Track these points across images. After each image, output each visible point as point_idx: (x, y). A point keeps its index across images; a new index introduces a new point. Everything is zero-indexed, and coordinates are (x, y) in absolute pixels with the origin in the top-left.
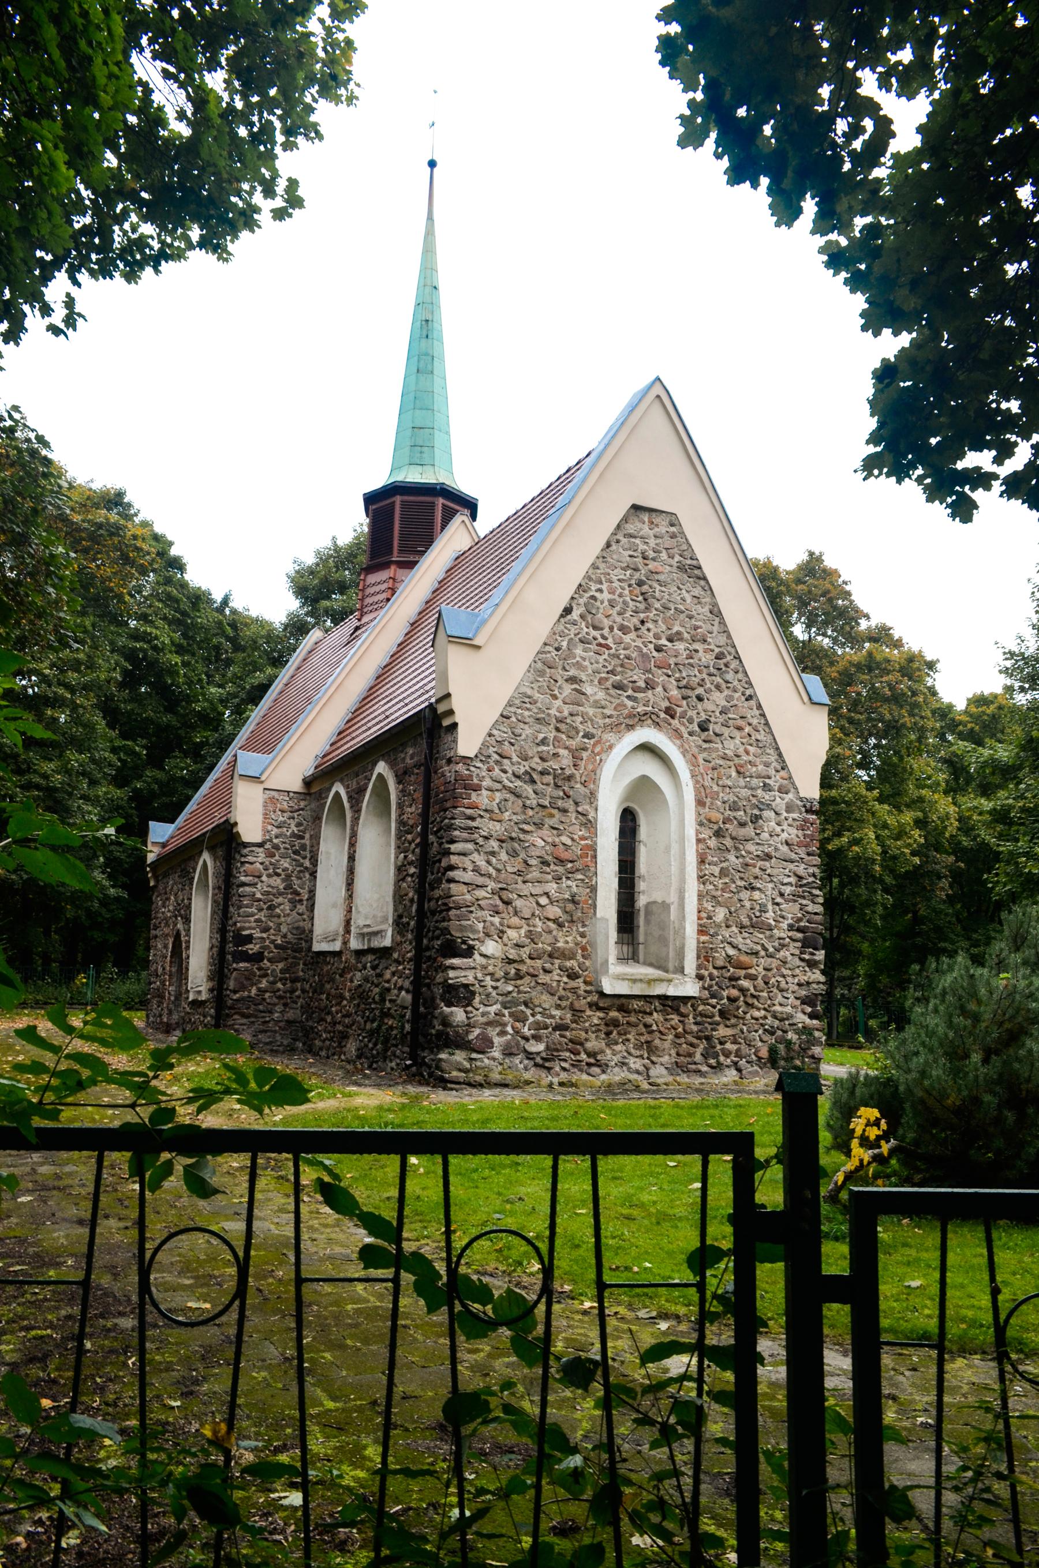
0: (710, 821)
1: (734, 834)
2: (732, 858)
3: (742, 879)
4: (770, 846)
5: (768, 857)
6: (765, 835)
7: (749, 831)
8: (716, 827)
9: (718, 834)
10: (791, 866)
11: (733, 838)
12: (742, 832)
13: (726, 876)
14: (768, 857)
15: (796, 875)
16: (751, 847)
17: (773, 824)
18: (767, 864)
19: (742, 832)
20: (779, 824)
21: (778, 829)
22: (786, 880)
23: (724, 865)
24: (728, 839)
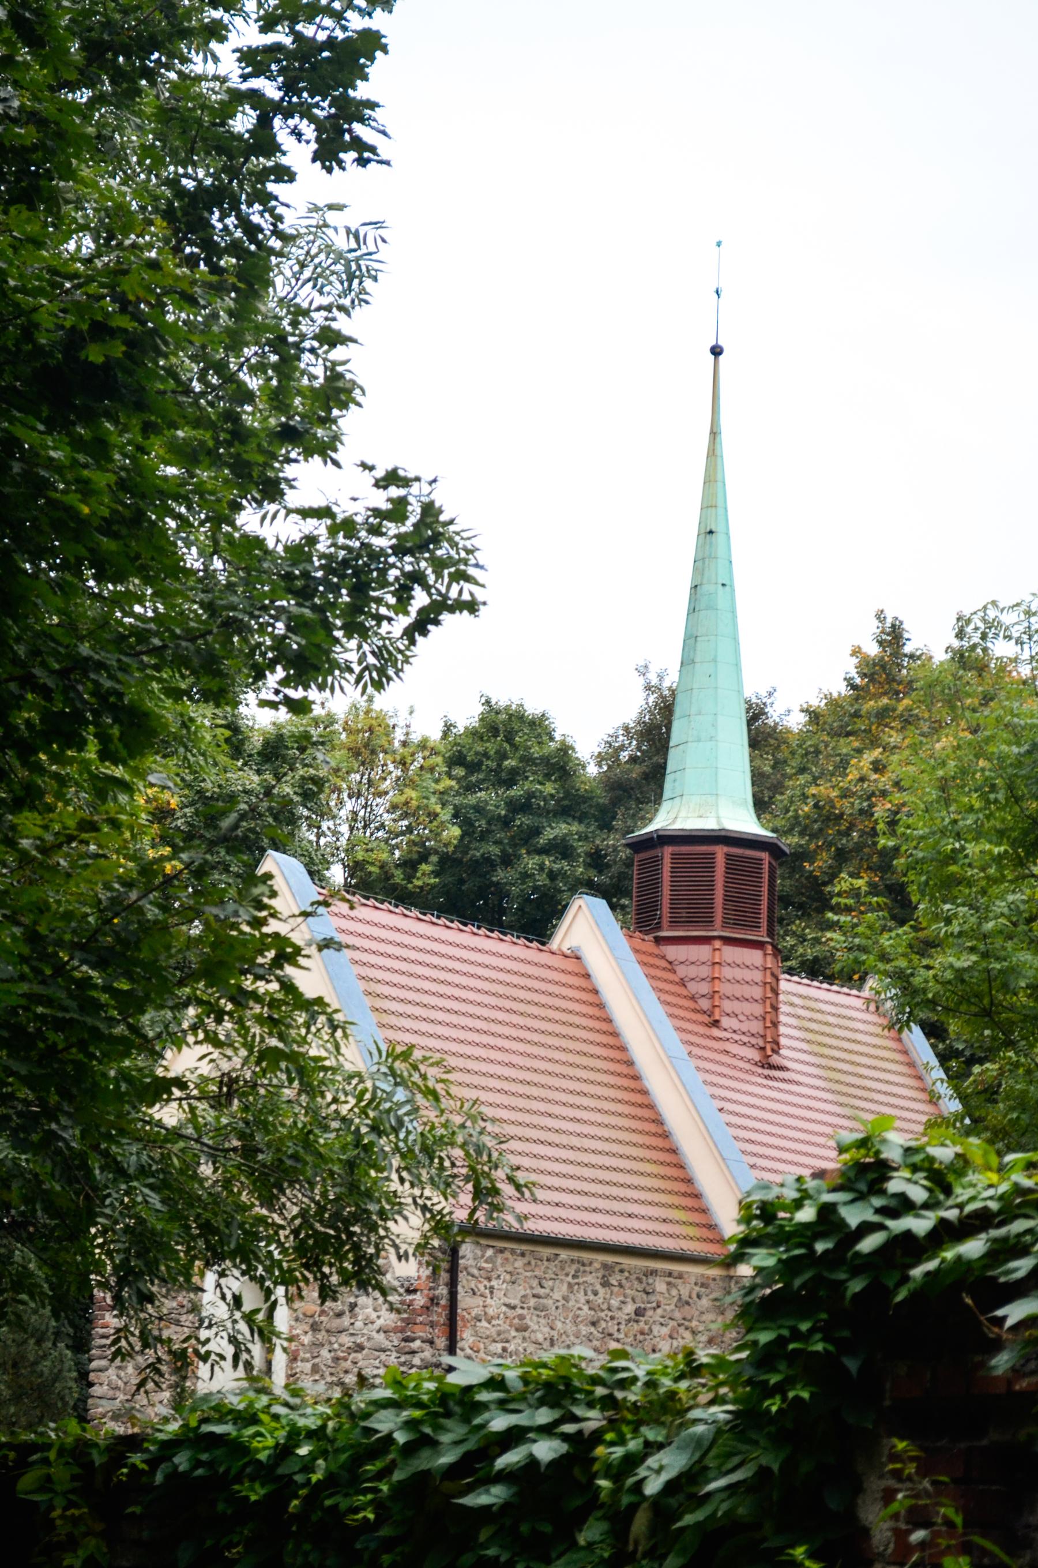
0: (305, 1315)
1: (328, 1326)
2: (324, 1353)
3: (332, 1374)
4: (363, 1335)
5: (360, 1348)
6: (359, 1324)
7: (346, 1321)
8: (311, 1321)
9: (315, 1328)
10: (383, 1356)
11: (328, 1331)
12: (336, 1323)
13: (317, 1372)
14: (360, 1348)
15: (386, 1366)
16: (346, 1340)
17: (370, 1310)
18: (359, 1356)
19: (336, 1323)
20: (375, 1310)
21: (374, 1315)
22: (376, 1372)
23: (316, 1360)
24: (323, 1333)
